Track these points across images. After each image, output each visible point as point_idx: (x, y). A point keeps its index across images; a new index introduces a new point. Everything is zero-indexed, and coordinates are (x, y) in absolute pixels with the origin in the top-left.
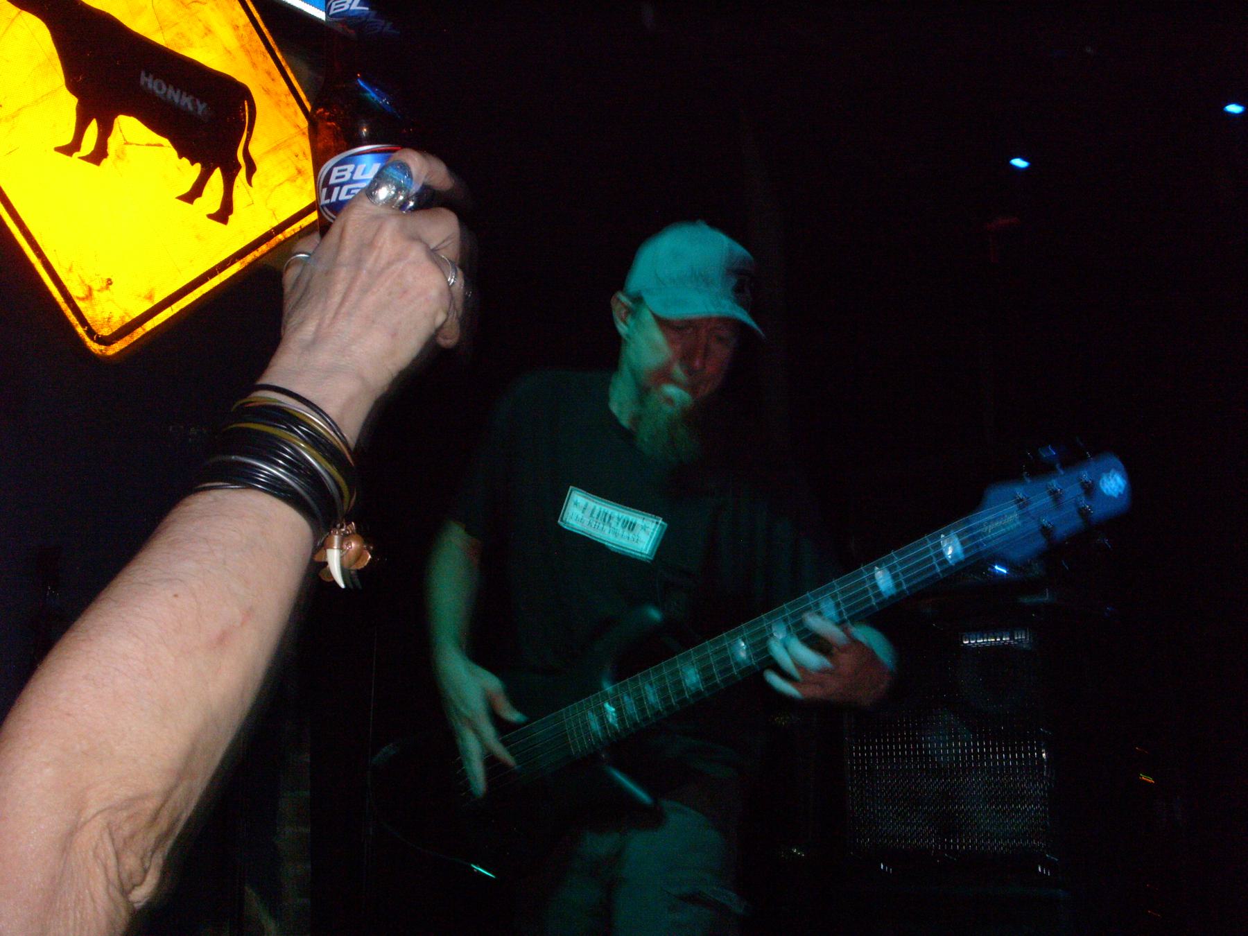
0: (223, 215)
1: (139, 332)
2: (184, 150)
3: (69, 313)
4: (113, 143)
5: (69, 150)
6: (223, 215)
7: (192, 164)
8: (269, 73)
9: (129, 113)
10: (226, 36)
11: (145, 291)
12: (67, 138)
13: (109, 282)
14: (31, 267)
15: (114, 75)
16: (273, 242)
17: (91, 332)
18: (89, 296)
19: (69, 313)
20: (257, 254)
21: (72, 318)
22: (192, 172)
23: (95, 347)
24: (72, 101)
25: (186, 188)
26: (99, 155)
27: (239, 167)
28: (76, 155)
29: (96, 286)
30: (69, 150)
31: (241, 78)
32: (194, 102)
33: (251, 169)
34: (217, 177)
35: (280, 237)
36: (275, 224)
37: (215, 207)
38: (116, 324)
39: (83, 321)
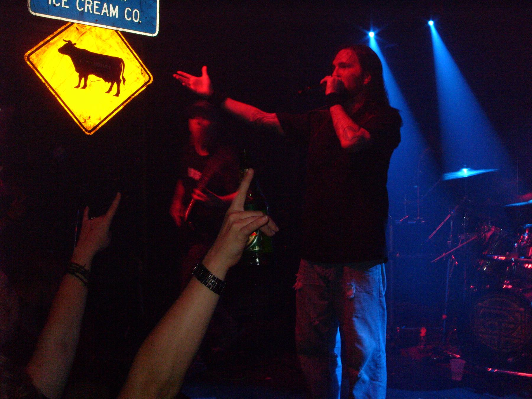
0: (117, 95)
1: (98, 128)
2: (107, 80)
3: (81, 126)
4: (88, 82)
5: (77, 87)
6: (117, 95)
8: (128, 53)
9: (91, 74)
10: (116, 46)
11: (99, 118)
12: (77, 84)
13: (90, 117)
14: (71, 117)
15: (88, 64)
16: (131, 99)
17: (86, 130)
18: (85, 121)
19: (81, 126)
20: (127, 102)
21: (82, 128)
23: (87, 133)
24: (78, 74)
25: (108, 89)
26: (85, 87)
27: (121, 81)
29: (86, 119)
30: (77, 87)
31: (120, 57)
33: (124, 80)
34: (115, 84)
35: (133, 97)
36: (132, 94)
37: (115, 93)
38: (92, 127)
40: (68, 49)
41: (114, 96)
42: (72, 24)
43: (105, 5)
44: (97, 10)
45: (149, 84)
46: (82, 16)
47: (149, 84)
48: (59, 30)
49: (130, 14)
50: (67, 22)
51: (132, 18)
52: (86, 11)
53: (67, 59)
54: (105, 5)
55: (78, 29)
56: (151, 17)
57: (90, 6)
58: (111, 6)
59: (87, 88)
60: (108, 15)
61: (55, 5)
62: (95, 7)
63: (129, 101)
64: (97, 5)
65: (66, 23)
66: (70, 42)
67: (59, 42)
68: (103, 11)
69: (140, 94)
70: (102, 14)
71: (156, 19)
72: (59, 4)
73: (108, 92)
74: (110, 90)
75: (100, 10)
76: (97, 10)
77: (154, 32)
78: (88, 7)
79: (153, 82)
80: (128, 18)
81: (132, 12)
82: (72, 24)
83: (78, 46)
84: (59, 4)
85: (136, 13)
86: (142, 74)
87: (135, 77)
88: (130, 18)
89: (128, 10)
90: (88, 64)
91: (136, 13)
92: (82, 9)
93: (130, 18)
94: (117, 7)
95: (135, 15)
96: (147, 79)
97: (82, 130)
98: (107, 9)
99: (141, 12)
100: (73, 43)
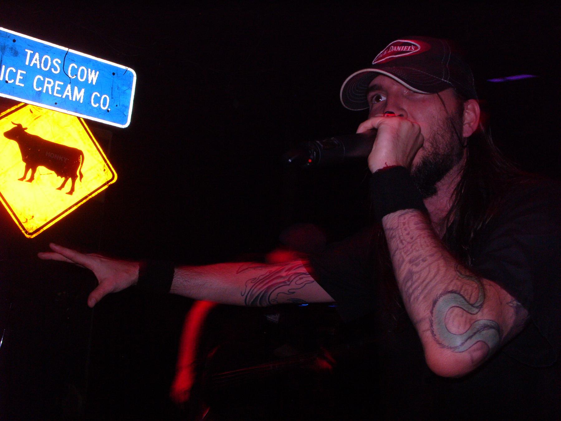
0: (71, 192)
1: (42, 231)
4: (36, 175)
5: (22, 179)
6: (71, 192)
7: (62, 177)
12: (22, 176)
13: (33, 217)
15: (40, 153)
16: (88, 199)
17: (26, 232)
18: (27, 221)
20: (82, 203)
21: (21, 229)
22: (61, 180)
23: (27, 236)
24: (24, 164)
25: (59, 186)
26: (32, 179)
27: (77, 176)
28: (24, 180)
29: (28, 219)
30: (22, 179)
31: (79, 149)
32: (63, 159)
34: (70, 180)
36: (89, 193)
38: (35, 229)
39: (24, 229)
40: (17, 134)
41: (67, 193)
42: (26, 105)
43: (69, 87)
44: (58, 92)
45: (111, 183)
46: (38, 97)
47: (111, 183)
48: (9, 111)
49: (97, 100)
50: (19, 103)
51: (100, 104)
52: (44, 91)
53: (14, 146)
54: (69, 87)
55: (32, 112)
56: (123, 105)
57: (50, 86)
58: (76, 88)
59: (33, 181)
60: (70, 99)
61: (7, 82)
62: (57, 88)
63: (85, 201)
64: (59, 85)
65: (17, 103)
66: (19, 126)
67: (8, 123)
68: (66, 93)
69: (99, 194)
70: (64, 97)
71: (128, 107)
72: (13, 81)
73: (60, 188)
74: (63, 186)
75: (61, 92)
76: (58, 92)
77: (124, 122)
78: (47, 88)
79: (117, 181)
80: (95, 103)
81: (100, 98)
82: (26, 105)
83: (31, 131)
84: (13, 81)
85: (105, 98)
86: (105, 170)
87: (97, 173)
88: (97, 105)
89: (96, 95)
90: (40, 153)
91: (105, 98)
92: (40, 89)
93: (97, 105)
94: (83, 90)
95: (104, 102)
96: (110, 176)
97: (21, 231)
98: (70, 91)
99: (112, 98)
100: (24, 127)
